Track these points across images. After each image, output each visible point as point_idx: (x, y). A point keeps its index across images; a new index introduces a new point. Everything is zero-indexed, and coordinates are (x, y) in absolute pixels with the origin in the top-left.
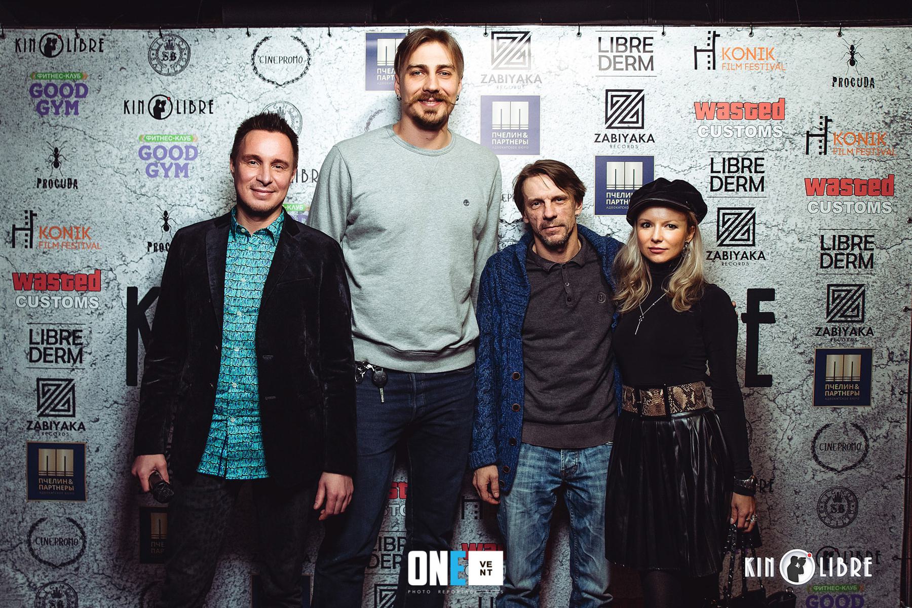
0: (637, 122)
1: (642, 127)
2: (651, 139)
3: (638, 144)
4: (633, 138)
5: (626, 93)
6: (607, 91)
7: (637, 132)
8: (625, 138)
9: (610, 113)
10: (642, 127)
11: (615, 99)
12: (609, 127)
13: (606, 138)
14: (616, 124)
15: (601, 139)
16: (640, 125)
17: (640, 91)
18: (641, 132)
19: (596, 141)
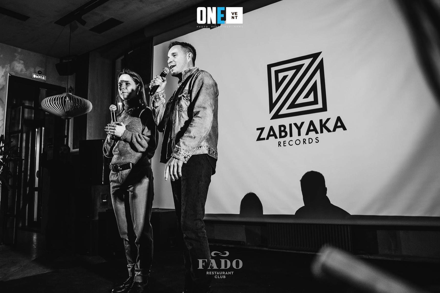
0: (316, 102)
1: (324, 109)
2: (340, 124)
3: (319, 135)
4: (312, 128)
5: (294, 64)
6: (269, 67)
7: (316, 118)
8: (299, 128)
9: (275, 96)
10: (324, 109)
11: (281, 76)
12: (276, 116)
13: (272, 133)
14: (284, 111)
15: (265, 135)
16: (320, 105)
17: (315, 56)
18: (323, 116)
19: (259, 139)
